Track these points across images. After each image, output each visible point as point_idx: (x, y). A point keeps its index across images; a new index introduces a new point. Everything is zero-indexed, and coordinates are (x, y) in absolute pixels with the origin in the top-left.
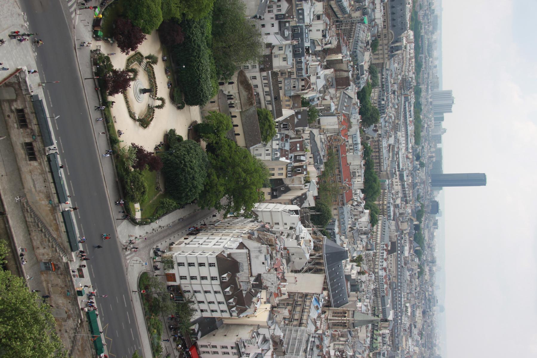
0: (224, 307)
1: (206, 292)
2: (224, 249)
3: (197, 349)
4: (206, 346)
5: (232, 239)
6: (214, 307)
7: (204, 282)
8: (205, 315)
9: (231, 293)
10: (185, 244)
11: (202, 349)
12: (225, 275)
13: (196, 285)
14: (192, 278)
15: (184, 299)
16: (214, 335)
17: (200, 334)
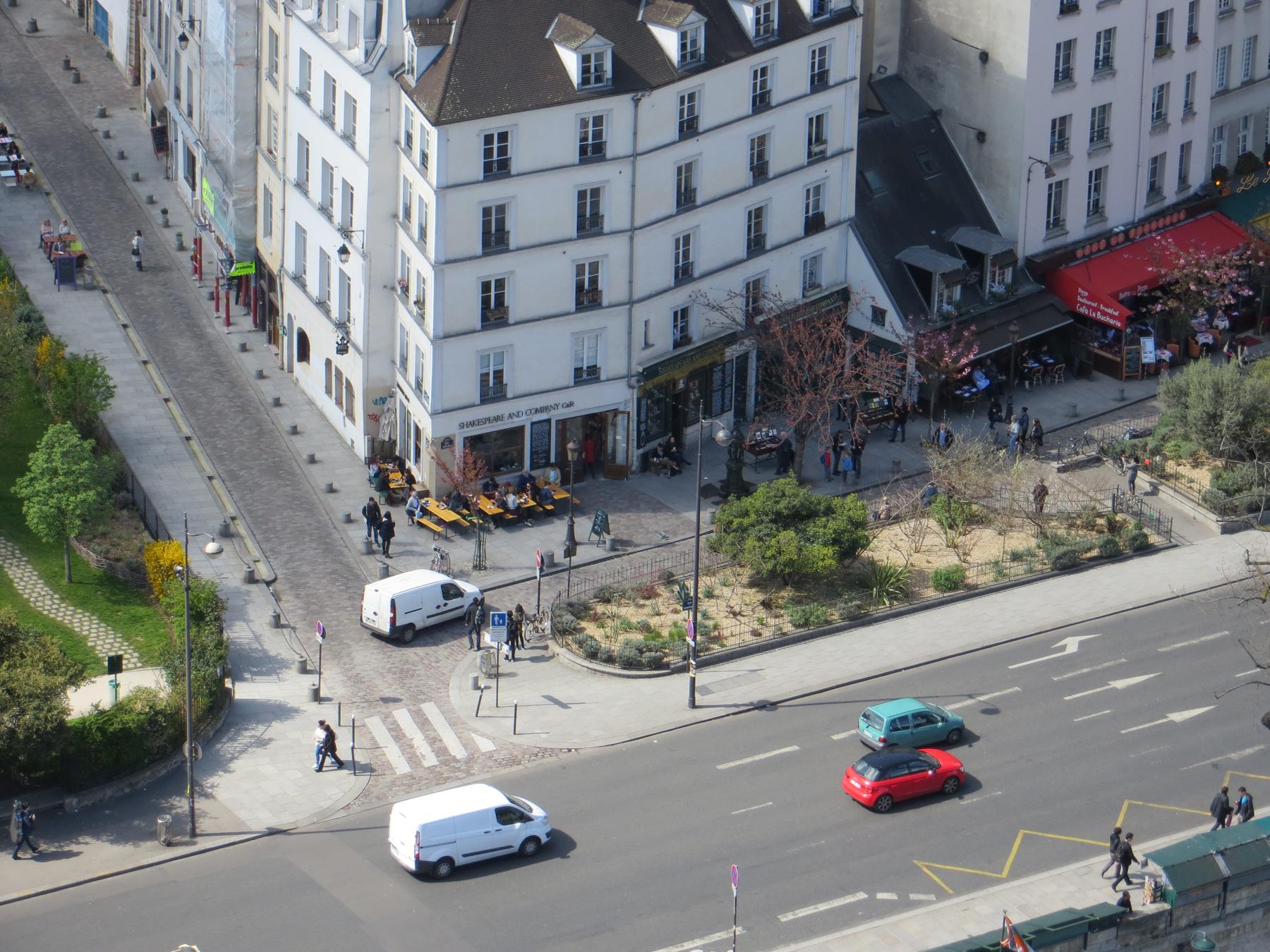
0: (789, 64)
1: (686, 199)
2: (382, 71)
3: (1066, 255)
4: (1056, 194)
5: (309, 15)
6: (787, 135)
7: (614, 213)
8: (841, 201)
9: (695, 21)
10: (342, 349)
11: (1077, 225)
12: (570, 60)
13: (635, 263)
14: (588, 296)
15: (732, 352)
16: (981, 137)
17: (966, 236)
